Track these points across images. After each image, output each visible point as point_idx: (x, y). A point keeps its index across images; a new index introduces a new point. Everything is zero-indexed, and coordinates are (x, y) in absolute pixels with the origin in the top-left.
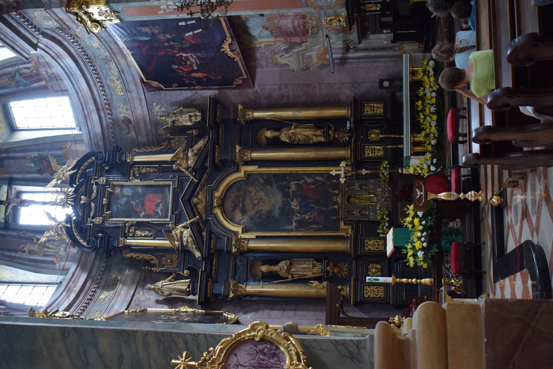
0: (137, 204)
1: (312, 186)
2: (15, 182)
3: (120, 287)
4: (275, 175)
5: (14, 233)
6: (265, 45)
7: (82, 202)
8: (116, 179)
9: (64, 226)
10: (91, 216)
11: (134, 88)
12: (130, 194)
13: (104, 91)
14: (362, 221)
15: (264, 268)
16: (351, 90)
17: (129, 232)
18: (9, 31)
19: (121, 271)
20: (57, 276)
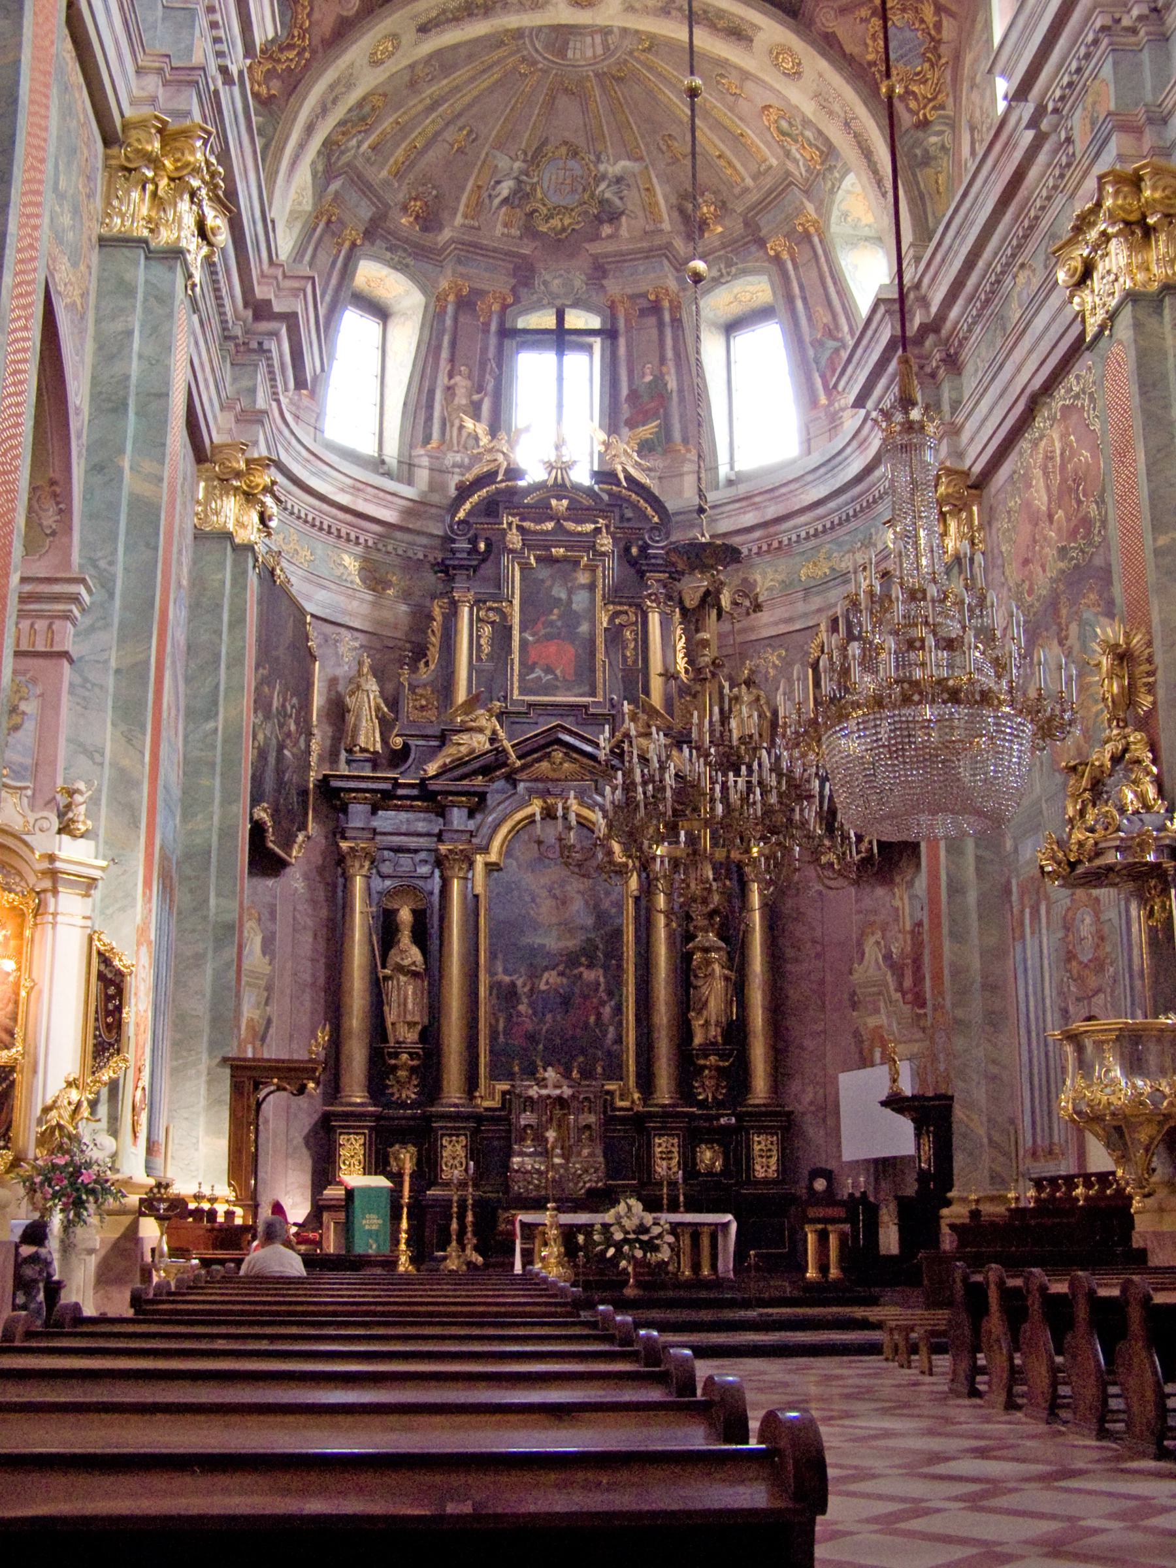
0: (551, 624)
1: (592, 1019)
2: (608, 342)
3: (369, 596)
4: (618, 933)
5: (492, 352)
6: (897, 909)
7: (554, 502)
8: (610, 571)
9: (499, 466)
10: (526, 524)
11: (814, 607)
12: (574, 606)
13: (807, 538)
14: (509, 1131)
15: (405, 915)
16: (811, 1103)
17: (490, 609)
18: (875, 356)
19: (406, 595)
20: (395, 454)
